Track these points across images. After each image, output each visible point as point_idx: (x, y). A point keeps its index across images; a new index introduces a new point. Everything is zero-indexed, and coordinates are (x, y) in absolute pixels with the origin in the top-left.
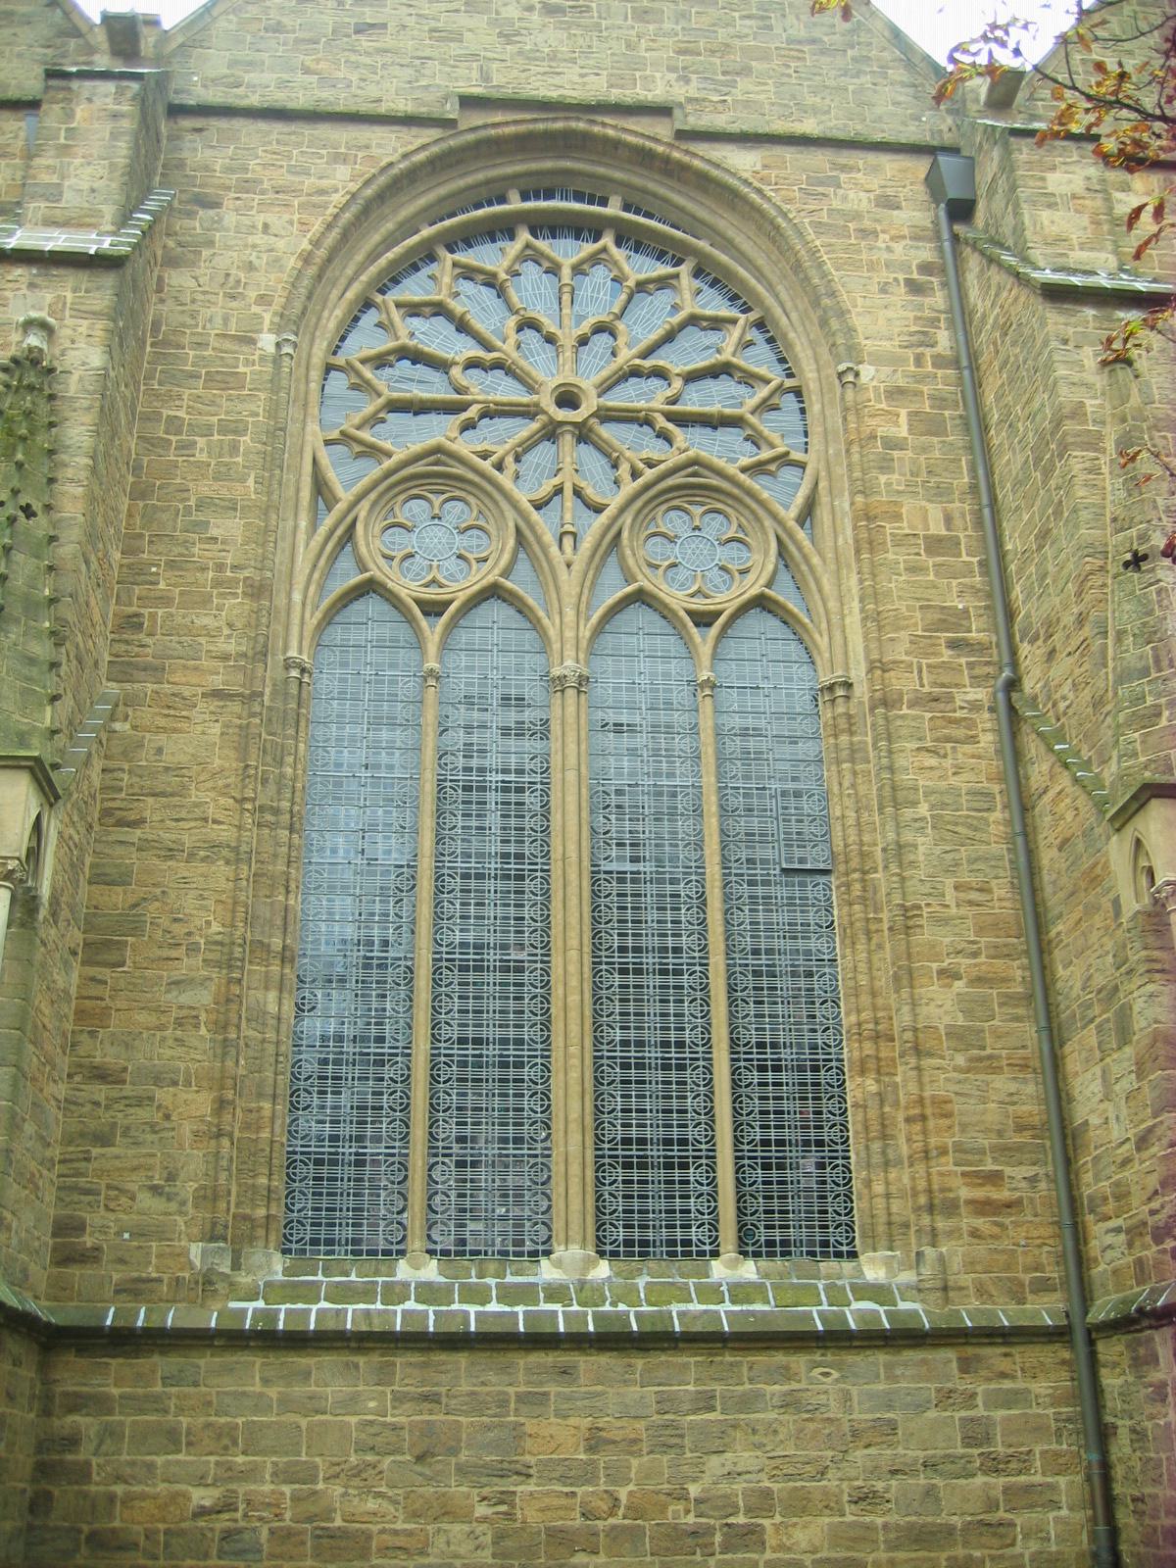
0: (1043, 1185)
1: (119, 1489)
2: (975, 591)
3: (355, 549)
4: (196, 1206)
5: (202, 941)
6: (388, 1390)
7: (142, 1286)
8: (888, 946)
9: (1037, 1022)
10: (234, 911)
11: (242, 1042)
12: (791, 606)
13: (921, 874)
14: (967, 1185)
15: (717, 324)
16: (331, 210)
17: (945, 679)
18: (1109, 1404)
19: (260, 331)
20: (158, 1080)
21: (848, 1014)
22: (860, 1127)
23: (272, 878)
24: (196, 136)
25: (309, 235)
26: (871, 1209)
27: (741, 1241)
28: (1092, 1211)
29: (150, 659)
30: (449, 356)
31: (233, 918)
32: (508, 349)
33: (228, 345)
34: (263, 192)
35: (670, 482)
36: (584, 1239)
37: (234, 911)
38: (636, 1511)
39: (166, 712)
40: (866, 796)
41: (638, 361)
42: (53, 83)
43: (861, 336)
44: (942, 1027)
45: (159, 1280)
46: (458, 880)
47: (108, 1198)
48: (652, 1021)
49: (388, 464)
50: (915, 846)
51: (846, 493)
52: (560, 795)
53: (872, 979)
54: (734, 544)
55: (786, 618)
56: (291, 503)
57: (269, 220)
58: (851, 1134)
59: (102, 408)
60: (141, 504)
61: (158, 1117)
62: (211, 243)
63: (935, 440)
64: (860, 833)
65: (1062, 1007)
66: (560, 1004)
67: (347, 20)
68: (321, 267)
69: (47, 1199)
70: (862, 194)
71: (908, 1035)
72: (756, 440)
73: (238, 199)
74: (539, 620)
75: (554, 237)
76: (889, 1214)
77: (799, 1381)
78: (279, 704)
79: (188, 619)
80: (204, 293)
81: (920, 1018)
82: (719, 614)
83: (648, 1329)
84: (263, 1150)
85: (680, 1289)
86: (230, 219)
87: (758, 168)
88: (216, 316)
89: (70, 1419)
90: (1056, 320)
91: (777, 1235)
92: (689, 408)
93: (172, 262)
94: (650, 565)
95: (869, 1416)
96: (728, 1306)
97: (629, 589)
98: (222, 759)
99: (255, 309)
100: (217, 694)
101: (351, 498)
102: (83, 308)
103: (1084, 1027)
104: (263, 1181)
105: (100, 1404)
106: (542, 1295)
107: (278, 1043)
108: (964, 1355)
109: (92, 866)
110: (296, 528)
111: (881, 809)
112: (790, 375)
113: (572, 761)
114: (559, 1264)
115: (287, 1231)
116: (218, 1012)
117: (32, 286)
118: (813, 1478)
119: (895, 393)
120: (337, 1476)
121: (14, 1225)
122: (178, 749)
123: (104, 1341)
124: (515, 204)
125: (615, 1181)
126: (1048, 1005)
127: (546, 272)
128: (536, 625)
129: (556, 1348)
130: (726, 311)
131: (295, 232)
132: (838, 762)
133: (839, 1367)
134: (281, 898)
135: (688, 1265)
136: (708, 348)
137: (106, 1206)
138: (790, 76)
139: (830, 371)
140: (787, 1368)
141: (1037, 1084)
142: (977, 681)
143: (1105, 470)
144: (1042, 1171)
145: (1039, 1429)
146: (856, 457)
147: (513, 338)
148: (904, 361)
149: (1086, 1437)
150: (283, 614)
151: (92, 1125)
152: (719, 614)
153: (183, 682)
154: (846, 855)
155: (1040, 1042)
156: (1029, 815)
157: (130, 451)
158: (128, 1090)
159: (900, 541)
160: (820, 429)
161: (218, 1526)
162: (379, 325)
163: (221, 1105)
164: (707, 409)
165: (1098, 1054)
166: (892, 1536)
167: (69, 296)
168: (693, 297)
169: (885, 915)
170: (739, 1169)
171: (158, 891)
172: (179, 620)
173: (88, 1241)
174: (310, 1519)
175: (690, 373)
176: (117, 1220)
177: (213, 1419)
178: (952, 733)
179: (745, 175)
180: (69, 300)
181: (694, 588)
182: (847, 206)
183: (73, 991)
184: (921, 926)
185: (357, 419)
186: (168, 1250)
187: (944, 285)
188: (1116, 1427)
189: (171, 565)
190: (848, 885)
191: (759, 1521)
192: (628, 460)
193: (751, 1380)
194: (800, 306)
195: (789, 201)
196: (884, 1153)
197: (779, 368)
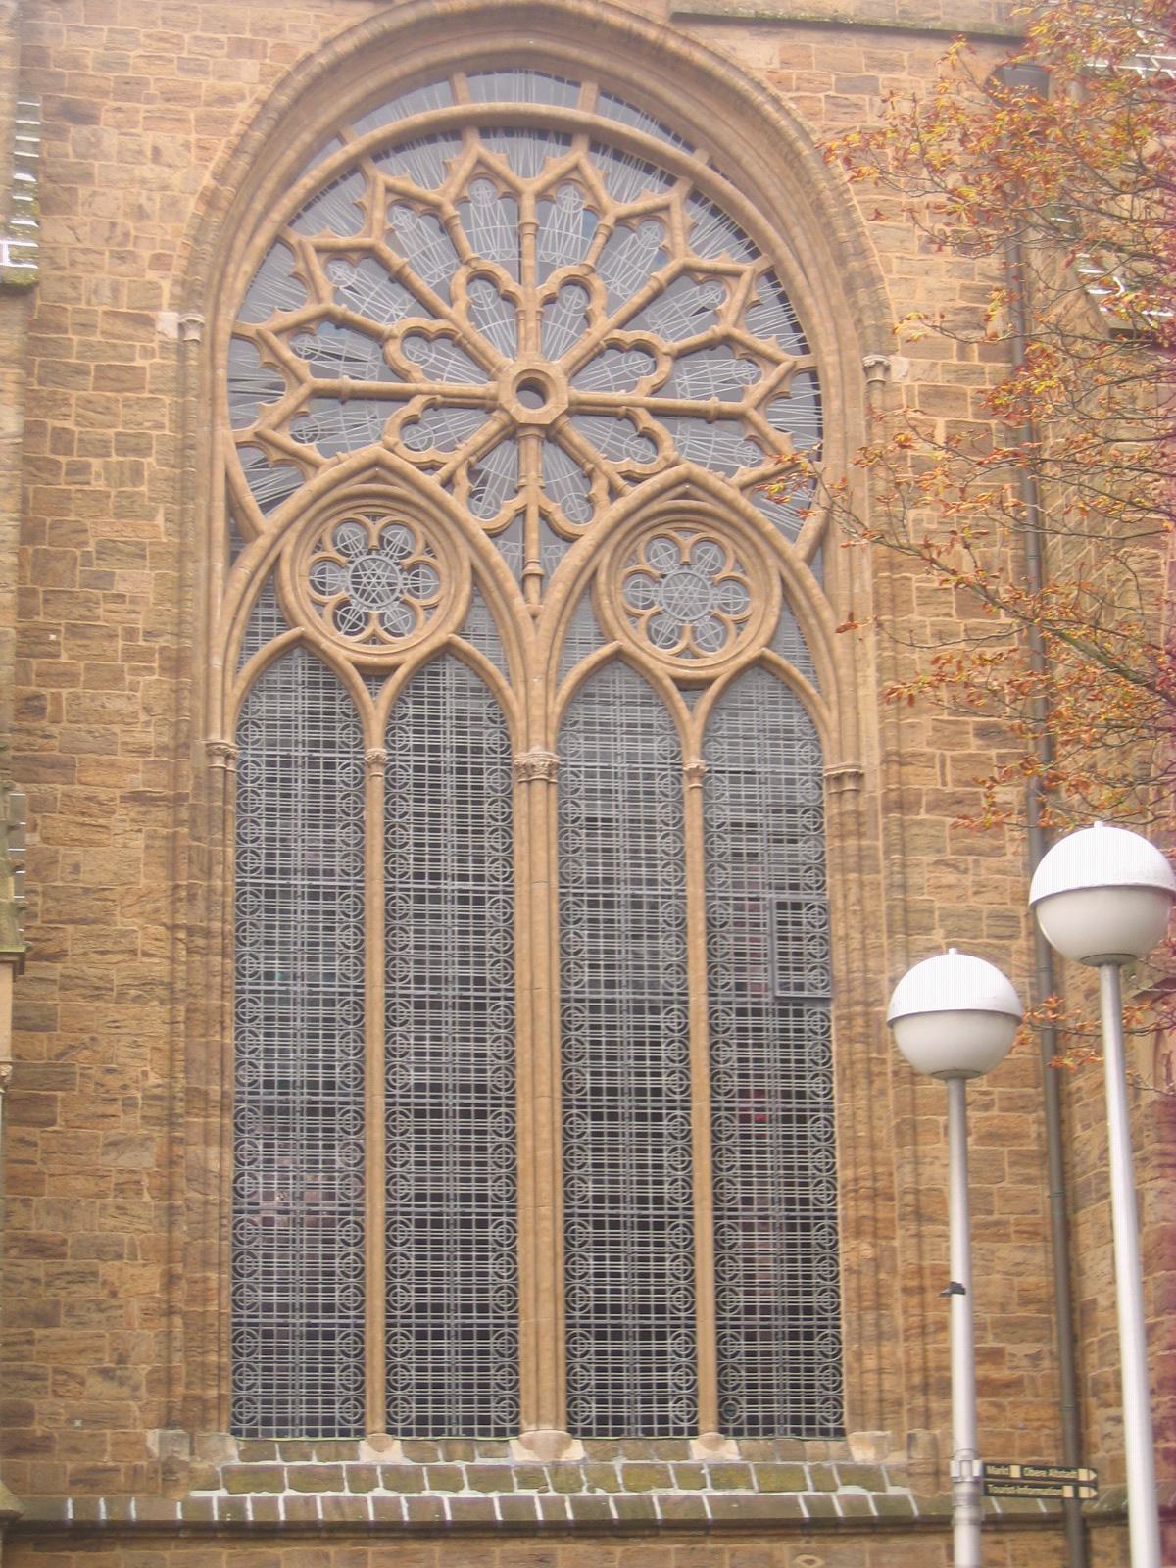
0: (1046, 1363)
4: (150, 1390)
5: (139, 1095)
8: (891, 1092)
10: (172, 1060)
16: (237, 128)
19: (157, 307)
20: (101, 1254)
21: (844, 1166)
22: (852, 1294)
23: (206, 1013)
26: (862, 1385)
27: (722, 1418)
28: (1094, 1394)
29: (56, 753)
30: (384, 326)
32: (457, 314)
33: (120, 327)
34: (150, 100)
36: (557, 1417)
37: (172, 1060)
39: (81, 819)
40: (873, 913)
43: (895, 316)
45: (116, 1470)
46: (411, 1010)
47: (54, 1383)
48: (628, 1174)
52: (526, 910)
53: (872, 1128)
54: (731, 585)
55: (789, 685)
56: (203, 538)
58: (842, 1300)
60: (31, 550)
61: (103, 1295)
64: (864, 960)
65: (1078, 1170)
66: (529, 1156)
72: (760, 441)
73: (119, 109)
76: (881, 1391)
78: (203, 802)
79: (98, 702)
80: (86, 251)
81: (924, 1178)
83: (629, 1516)
84: (212, 1325)
85: (658, 1472)
86: (111, 140)
87: (776, 65)
94: (630, 615)
96: (708, 1492)
97: (606, 649)
98: (150, 879)
99: (151, 276)
100: (137, 797)
101: (275, 531)
104: (213, 1358)
106: (515, 1479)
107: (221, 1203)
110: (210, 571)
112: (805, 350)
113: (541, 871)
114: (530, 1445)
115: (237, 1410)
119: (934, 396)
123: (66, 1534)
125: (587, 1353)
129: (533, 1536)
130: (724, 262)
131: (193, 159)
132: (844, 870)
133: (823, 1554)
134: (217, 1038)
135: (665, 1444)
136: (703, 309)
137: (54, 1391)
141: (1046, 1252)
143: (1164, 571)
148: (944, 351)
151: (33, 1303)
152: (708, 682)
154: (849, 982)
155: (1052, 1208)
160: (839, 436)
163: (170, 1280)
164: (702, 404)
170: (720, 1338)
171: (86, 1037)
172: (87, 703)
173: (38, 1429)
179: (759, 76)
185: (275, 419)
189: (73, 631)
190: (849, 1018)
192: (605, 474)
195: (813, 115)
196: (877, 1325)
197: (793, 338)
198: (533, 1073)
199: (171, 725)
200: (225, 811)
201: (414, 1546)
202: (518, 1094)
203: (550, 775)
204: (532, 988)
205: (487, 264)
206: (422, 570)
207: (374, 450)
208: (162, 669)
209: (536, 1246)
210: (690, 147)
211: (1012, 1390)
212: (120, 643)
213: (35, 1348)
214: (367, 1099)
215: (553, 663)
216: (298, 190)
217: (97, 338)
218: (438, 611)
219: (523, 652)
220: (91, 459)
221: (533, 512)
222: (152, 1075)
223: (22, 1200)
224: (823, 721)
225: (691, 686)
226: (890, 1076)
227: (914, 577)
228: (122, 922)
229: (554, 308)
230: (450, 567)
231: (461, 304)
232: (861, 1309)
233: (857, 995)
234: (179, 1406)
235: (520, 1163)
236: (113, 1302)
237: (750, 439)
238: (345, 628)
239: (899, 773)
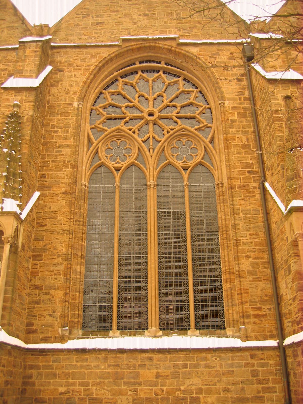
0: (272, 310)
1: (42, 388)
2: (255, 158)
3: (98, 155)
4: (60, 319)
5: (61, 254)
6: (106, 363)
7: (47, 339)
8: (233, 250)
9: (271, 268)
11: (71, 279)
12: (208, 164)
13: (240, 231)
14: (252, 310)
15: (189, 93)
16: (91, 70)
17: (247, 181)
18: (289, 366)
19: (74, 102)
20: (51, 288)
21: (223, 267)
22: (226, 296)
23: (78, 238)
24: (58, 54)
25: (85, 77)
26: (229, 317)
31: (69, 248)
32: (136, 102)
33: (66, 106)
35: (177, 134)
38: (168, 393)
40: (227, 212)
41: (169, 103)
42: (21, 44)
43: (225, 94)
44: (246, 271)
45: (51, 337)
47: (39, 317)
49: (106, 133)
50: (239, 224)
51: (222, 134)
53: (229, 258)
57: (76, 74)
59: (32, 125)
60: (45, 147)
61: (51, 297)
62: (61, 80)
63: (244, 119)
64: (225, 222)
65: (277, 264)
67: (94, 22)
68: (88, 85)
69: (24, 318)
70: (225, 57)
71: (237, 273)
73: (68, 69)
74: (144, 171)
75: (147, 73)
76: (233, 318)
77: (209, 361)
79: (57, 175)
80: (60, 93)
81: (241, 268)
84: (77, 305)
86: (66, 74)
87: (198, 52)
88: (63, 99)
89: (30, 371)
90: (271, 88)
91: (205, 324)
92: (181, 115)
93: (52, 86)
94: (172, 155)
95: (227, 369)
97: (167, 162)
98: (65, 209)
99: (73, 96)
100: (64, 193)
101: (97, 142)
102: (27, 100)
103: (281, 270)
104: (77, 312)
105: (38, 367)
107: (80, 278)
108: (251, 354)
109: (35, 236)
110: (83, 150)
111: (231, 215)
112: (208, 104)
113: (152, 206)
116: (65, 271)
117: (15, 96)
119: (234, 108)
120: (94, 385)
121: (14, 325)
122: (55, 207)
124: (138, 65)
126: (273, 264)
128: (143, 172)
132: (220, 203)
133: (219, 357)
134: (81, 243)
136: (187, 99)
138: (206, 27)
139: (218, 103)
140: (206, 358)
142: (255, 181)
143: (284, 126)
144: (271, 306)
145: (271, 373)
146: (224, 125)
147: (137, 99)
148: (236, 99)
149: (283, 375)
150: (81, 172)
151: (35, 299)
152: (189, 167)
153: (55, 190)
155: (271, 274)
156: (269, 215)
157: (42, 134)
158: (44, 291)
159: (235, 146)
160: (215, 118)
161: (65, 397)
162: (104, 98)
163: (66, 294)
164: (186, 114)
165: (284, 277)
166: (233, 400)
167: (24, 97)
168: (182, 86)
169: (232, 242)
172: (55, 175)
173: (34, 328)
174: (88, 395)
175: (182, 105)
176: (41, 323)
177: (65, 371)
178: (249, 194)
180: (24, 99)
181: (184, 160)
182: (221, 60)
183: (30, 267)
184: (241, 245)
186: (53, 330)
187: (246, 79)
188: (290, 372)
189: (53, 161)
190: (223, 235)
191: (199, 396)
192: (166, 129)
193: (197, 361)
194: (210, 87)
195: (206, 60)
196: (232, 303)
197: (205, 103)
199: (72, 179)
200: (85, 197)
201: (119, 355)
203: (154, 186)
205: (142, 93)
211: (265, 317)
213: (35, 309)
215: (155, 164)
217: (62, 108)
222: (64, 250)
223: (34, 277)
224: (214, 173)
225: (185, 169)
226: (232, 246)
227: (232, 142)
232: (228, 299)
233: (224, 229)
236: (53, 299)
239: (231, 182)
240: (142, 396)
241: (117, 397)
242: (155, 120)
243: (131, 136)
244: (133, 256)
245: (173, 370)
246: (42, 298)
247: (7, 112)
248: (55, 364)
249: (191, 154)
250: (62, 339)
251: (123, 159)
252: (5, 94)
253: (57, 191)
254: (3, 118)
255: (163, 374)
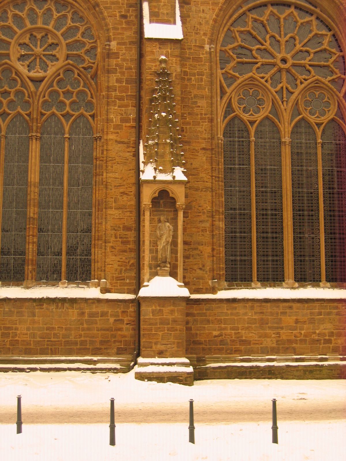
1: (198, 332)
4: (210, 272)
10: (212, 204)
16: (220, 5)
19: (205, 44)
20: (199, 244)
32: (267, 45)
33: (197, 49)
35: (311, 85)
38: (305, 336)
39: (192, 154)
52: (285, 172)
57: (204, 9)
62: (189, 16)
66: (286, 224)
72: (332, 72)
78: (217, 150)
80: (189, 32)
82: (323, 123)
86: (194, 8)
94: (305, 109)
97: (301, 117)
98: (207, 166)
99: (203, 37)
100: (204, 149)
101: (230, 92)
110: (217, 100)
112: (341, 51)
118: (342, 330)
120: (243, 329)
127: (276, 19)
130: (324, 32)
136: (319, 43)
152: (323, 123)
158: (192, 246)
161: (219, 339)
163: (213, 249)
167: (169, 51)
174: (238, 338)
176: (192, 276)
185: (229, 68)
189: (189, 114)
193: (330, 309)
197: (338, 49)
198: (287, 207)
201: (264, 304)
202: (283, 211)
204: (286, 189)
205: (273, 34)
206: (261, 100)
207: (251, 74)
208: (208, 122)
209: (288, 243)
210: (316, 7)
212: (199, 116)
214: (252, 212)
216: (233, 18)
217: (192, 51)
218: (265, 109)
219: (283, 117)
220: (192, 77)
221: (284, 87)
228: (202, 175)
229: (288, 43)
230: (267, 99)
231: (268, 42)
234: (215, 275)
235: (284, 225)
236: (201, 254)
237: (330, 71)
238: (245, 112)
240: (284, 338)
241: (263, 339)
242: (289, 68)
243: (265, 86)
244: (269, 212)
245: (310, 317)
246: (191, 253)
247: (154, 68)
248: (208, 312)
249: (324, 108)
250: (213, 291)
251: (256, 110)
252: (149, 46)
253: (197, 146)
254: (151, 74)
255: (301, 320)
